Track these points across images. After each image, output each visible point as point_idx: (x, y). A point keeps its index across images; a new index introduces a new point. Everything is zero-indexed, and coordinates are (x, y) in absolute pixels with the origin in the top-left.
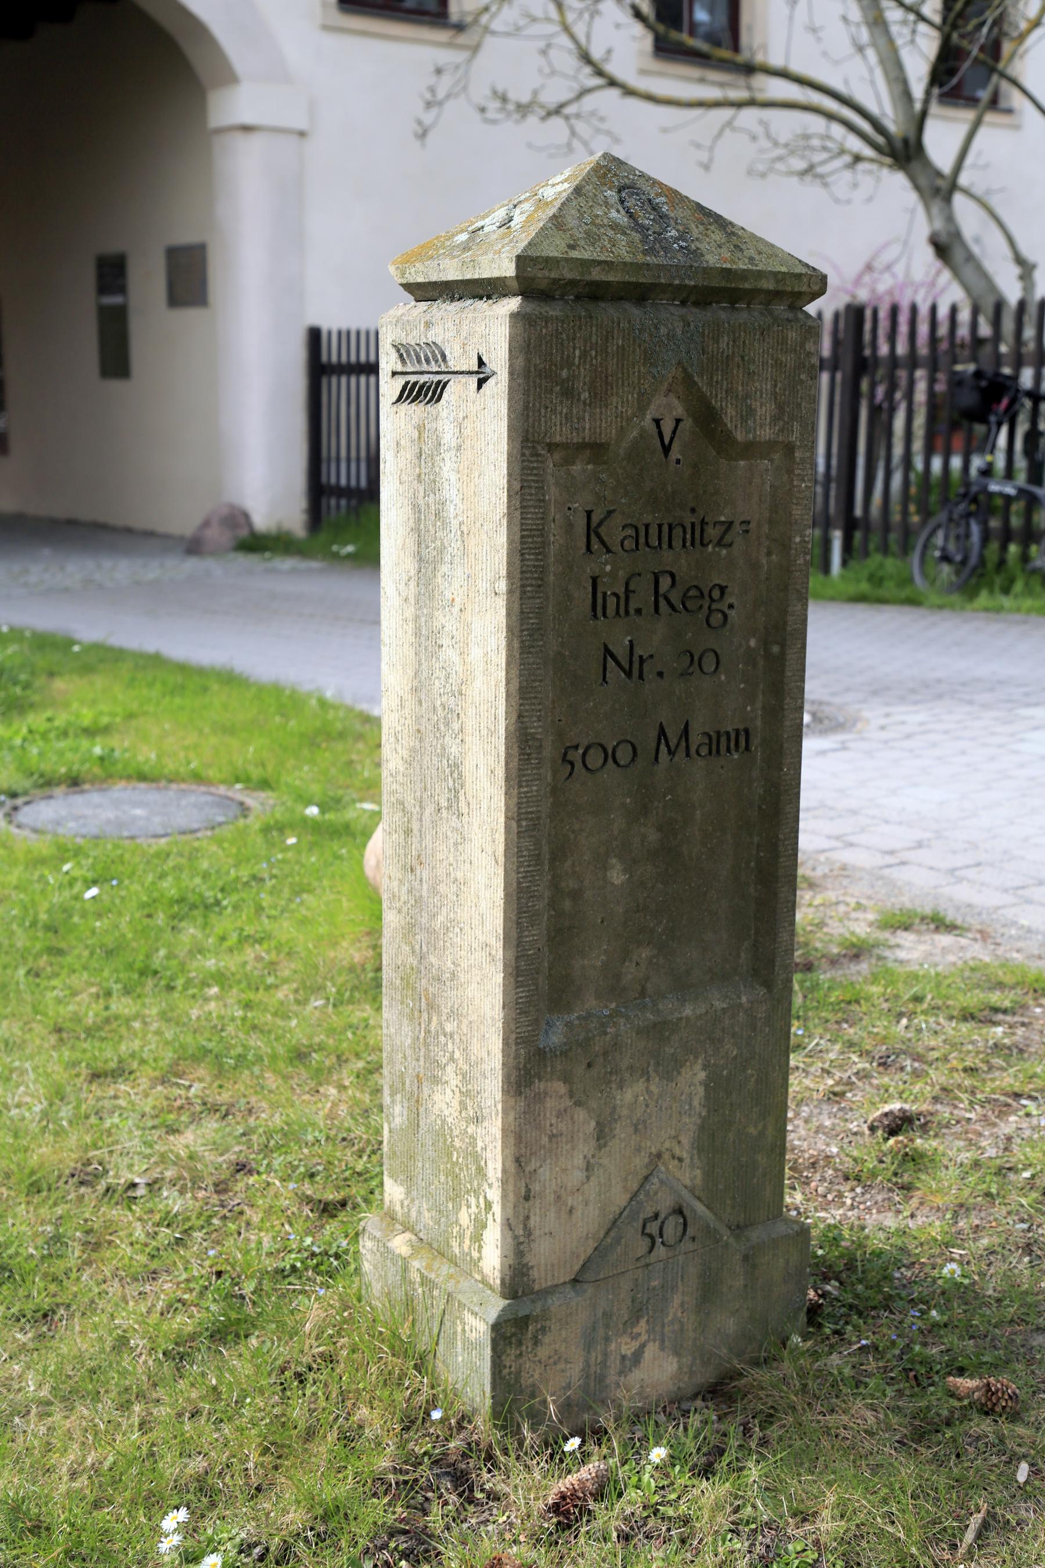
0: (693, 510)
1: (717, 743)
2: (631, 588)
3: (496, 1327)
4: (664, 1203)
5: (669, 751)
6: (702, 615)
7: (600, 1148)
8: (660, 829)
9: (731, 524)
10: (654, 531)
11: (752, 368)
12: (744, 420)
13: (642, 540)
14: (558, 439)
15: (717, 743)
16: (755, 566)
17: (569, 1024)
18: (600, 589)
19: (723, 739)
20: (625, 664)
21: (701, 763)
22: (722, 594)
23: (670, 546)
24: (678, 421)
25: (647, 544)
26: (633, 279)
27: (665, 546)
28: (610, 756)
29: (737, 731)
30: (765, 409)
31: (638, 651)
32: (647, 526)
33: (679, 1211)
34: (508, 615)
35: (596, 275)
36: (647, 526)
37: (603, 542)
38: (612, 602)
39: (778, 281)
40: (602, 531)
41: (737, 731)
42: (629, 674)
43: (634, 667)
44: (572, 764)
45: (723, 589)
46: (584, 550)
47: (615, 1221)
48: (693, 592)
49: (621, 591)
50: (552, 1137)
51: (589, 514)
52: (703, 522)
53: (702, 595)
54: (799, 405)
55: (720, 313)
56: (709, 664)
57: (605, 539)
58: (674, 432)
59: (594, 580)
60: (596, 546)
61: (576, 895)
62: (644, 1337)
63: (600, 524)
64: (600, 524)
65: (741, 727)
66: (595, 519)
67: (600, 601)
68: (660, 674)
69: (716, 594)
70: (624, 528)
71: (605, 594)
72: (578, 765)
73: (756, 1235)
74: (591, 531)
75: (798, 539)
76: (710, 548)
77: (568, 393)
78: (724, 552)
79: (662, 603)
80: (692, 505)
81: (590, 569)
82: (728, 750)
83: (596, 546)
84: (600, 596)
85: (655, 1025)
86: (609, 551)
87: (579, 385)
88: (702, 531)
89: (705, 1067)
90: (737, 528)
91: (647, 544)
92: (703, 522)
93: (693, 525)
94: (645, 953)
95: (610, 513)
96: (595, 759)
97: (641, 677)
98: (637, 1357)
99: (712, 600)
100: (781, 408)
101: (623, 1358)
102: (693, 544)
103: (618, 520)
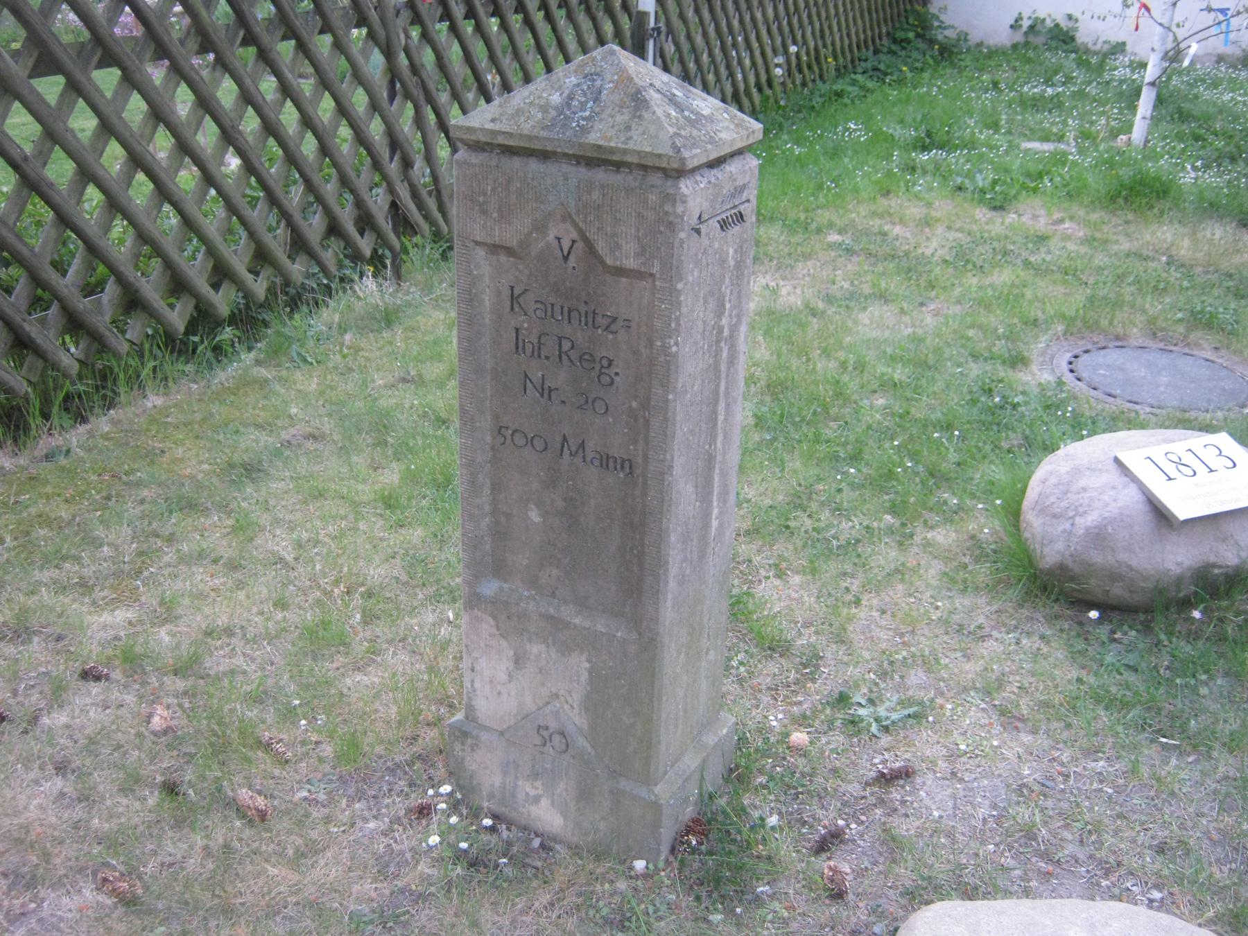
0: (586, 303)
1: (605, 461)
4: (553, 725)
5: (571, 454)
6: (594, 374)
8: (565, 500)
9: (615, 319)
10: (557, 308)
13: (549, 313)
14: (478, 239)
15: (605, 461)
16: (636, 353)
17: (501, 589)
18: (520, 338)
20: (539, 387)
22: (610, 365)
24: (574, 242)
25: (553, 316)
29: (623, 461)
30: (630, 247)
31: (547, 384)
33: (562, 734)
35: (501, 140)
38: (529, 347)
39: (640, 158)
41: (623, 461)
42: (542, 395)
43: (546, 392)
45: (610, 362)
46: (508, 310)
51: (512, 288)
52: (594, 313)
53: (594, 361)
54: (659, 249)
55: (600, 175)
58: (571, 248)
59: (517, 330)
61: (508, 516)
62: (541, 792)
63: (520, 296)
65: (626, 457)
66: (516, 292)
67: (521, 345)
69: (605, 363)
73: (624, 784)
74: (513, 298)
76: (600, 331)
77: (484, 212)
78: (611, 337)
81: (513, 323)
85: (552, 617)
89: (589, 661)
93: (586, 313)
94: (555, 572)
96: (520, 440)
98: (536, 800)
101: (527, 794)
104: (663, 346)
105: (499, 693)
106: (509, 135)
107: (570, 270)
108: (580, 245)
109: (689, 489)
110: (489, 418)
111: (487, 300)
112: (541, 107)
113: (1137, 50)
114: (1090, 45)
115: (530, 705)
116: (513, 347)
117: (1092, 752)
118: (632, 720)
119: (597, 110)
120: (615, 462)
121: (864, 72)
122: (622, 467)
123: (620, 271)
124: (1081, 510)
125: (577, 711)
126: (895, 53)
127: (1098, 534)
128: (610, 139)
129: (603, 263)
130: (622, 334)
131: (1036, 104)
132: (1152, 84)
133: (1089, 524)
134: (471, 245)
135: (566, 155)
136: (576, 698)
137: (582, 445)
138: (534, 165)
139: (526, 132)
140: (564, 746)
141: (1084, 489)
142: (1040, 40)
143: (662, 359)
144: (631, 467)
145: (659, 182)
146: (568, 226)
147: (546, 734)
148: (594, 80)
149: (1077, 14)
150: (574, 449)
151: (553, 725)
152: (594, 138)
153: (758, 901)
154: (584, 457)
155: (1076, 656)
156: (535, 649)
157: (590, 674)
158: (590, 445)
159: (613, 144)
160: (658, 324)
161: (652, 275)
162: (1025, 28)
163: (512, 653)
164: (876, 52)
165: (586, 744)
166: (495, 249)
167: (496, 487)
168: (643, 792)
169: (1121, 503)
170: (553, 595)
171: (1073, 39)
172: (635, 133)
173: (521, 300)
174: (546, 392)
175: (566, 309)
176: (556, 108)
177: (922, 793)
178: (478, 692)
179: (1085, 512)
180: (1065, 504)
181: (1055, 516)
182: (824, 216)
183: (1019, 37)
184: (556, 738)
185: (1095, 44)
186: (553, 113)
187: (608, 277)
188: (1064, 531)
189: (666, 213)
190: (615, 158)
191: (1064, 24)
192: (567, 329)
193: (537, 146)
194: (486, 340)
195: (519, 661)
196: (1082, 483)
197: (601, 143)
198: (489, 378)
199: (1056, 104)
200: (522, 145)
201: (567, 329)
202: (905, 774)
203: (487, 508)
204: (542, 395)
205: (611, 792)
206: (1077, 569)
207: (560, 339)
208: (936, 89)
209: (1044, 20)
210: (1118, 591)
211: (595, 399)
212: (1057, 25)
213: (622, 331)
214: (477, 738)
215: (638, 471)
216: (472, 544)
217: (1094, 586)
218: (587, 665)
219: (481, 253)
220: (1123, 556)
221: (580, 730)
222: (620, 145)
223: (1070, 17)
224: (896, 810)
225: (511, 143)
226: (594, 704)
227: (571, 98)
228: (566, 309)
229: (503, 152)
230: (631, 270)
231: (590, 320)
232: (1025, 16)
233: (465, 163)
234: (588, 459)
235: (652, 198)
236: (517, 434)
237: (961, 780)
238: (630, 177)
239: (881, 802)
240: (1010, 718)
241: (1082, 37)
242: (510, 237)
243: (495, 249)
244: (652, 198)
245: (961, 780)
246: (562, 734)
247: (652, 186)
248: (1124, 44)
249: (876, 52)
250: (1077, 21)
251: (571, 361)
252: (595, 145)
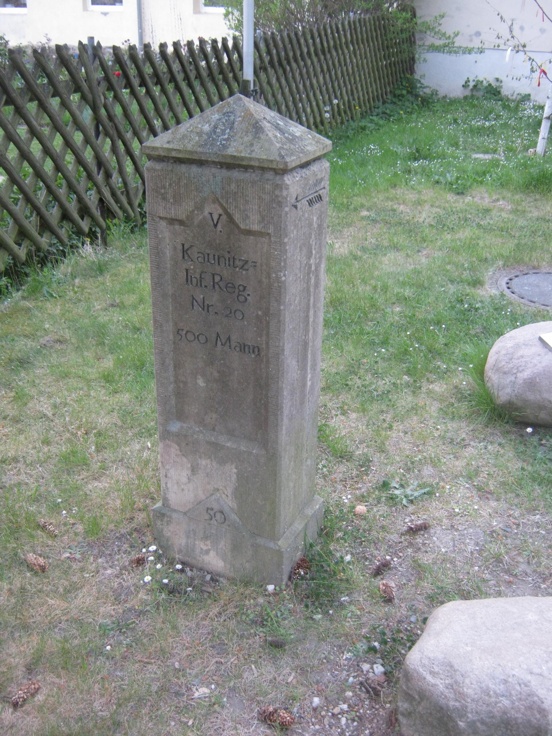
0: (229, 252)
1: (243, 348)
5: (222, 344)
7: (193, 475)
10: (211, 257)
11: (247, 198)
12: (244, 220)
13: (206, 260)
14: (161, 215)
15: (243, 348)
16: (260, 282)
17: (182, 427)
18: (189, 274)
20: (201, 304)
22: (244, 290)
23: (219, 264)
24: (220, 215)
25: (208, 261)
26: (190, 157)
29: (254, 348)
31: (207, 302)
32: (208, 254)
33: (222, 512)
35: (174, 154)
36: (208, 254)
37: (189, 256)
39: (260, 163)
42: (203, 309)
43: (206, 307)
45: (245, 288)
47: (200, 502)
48: (230, 285)
49: (198, 277)
50: (174, 462)
51: (183, 245)
52: (234, 258)
53: (235, 287)
54: (272, 218)
55: (236, 174)
56: (239, 315)
58: (219, 219)
59: (187, 270)
61: (185, 383)
62: (210, 547)
63: (188, 249)
65: (256, 345)
66: (186, 247)
67: (189, 279)
70: (198, 253)
73: (260, 541)
74: (184, 251)
75: (274, 275)
76: (237, 269)
77: (164, 199)
78: (244, 272)
80: (229, 250)
82: (249, 352)
83: (186, 258)
84: (189, 277)
85: (213, 443)
86: (192, 261)
87: (169, 196)
88: (234, 262)
89: (236, 468)
90: (250, 264)
91: (208, 261)
94: (214, 416)
96: (190, 337)
97: (208, 312)
98: (207, 552)
100: (263, 219)
101: (202, 549)
102: (229, 265)
103: (195, 250)
104: (277, 277)
105: (183, 490)
106: (179, 151)
107: (218, 232)
108: (224, 217)
109: (294, 363)
110: (171, 324)
111: (168, 253)
112: (198, 133)
113: (536, 99)
114: (509, 96)
115: (202, 497)
117: (532, 510)
118: (263, 503)
119: (232, 134)
120: (249, 348)
121: (377, 115)
122: (253, 352)
123: (249, 232)
124: (520, 369)
125: (230, 498)
126: (395, 103)
127: (531, 383)
128: (241, 152)
129: (238, 227)
130: (251, 270)
131: (480, 131)
132: (548, 118)
133: (525, 377)
134: (158, 219)
135: (214, 162)
136: (229, 491)
137: (229, 339)
138: (195, 169)
139: (189, 149)
140: (223, 520)
141: (522, 357)
142: (480, 94)
143: (276, 285)
144: (258, 351)
145: (271, 177)
146: (217, 206)
147: (212, 513)
148: (229, 116)
149: (501, 78)
150: (224, 341)
151: (216, 507)
152: (231, 151)
153: (342, 606)
154: (230, 346)
155: (519, 455)
156: (203, 462)
157: (237, 476)
158: (233, 338)
159: (242, 155)
160: (273, 264)
161: (268, 234)
162: (471, 87)
163: (190, 465)
164: (384, 103)
165: (236, 517)
166: (172, 221)
167: (177, 366)
168: (272, 545)
169: (544, 364)
170: (214, 430)
171: (499, 92)
172: (256, 148)
173: (189, 252)
174: (206, 308)
175: (216, 257)
176: (207, 134)
177: (434, 538)
178: (170, 490)
179: (523, 370)
180: (511, 365)
181: (505, 373)
182: (357, 201)
183: (468, 93)
184: (218, 515)
185: (512, 95)
186: (205, 137)
187: (242, 237)
188: (511, 381)
189: (277, 196)
190: (244, 163)
191: (494, 84)
192: (218, 269)
193: (195, 157)
194: (168, 277)
195: (194, 470)
196: (520, 353)
197: (235, 154)
198: (170, 300)
199: (491, 131)
200: (187, 157)
201: (218, 269)
202: (424, 527)
203: (172, 379)
204: (203, 309)
205: (252, 545)
206: (519, 404)
207: (213, 275)
208: (420, 123)
209: (482, 81)
210: (543, 416)
211: (235, 311)
212: (490, 85)
214: (170, 517)
215: (263, 354)
216: (163, 400)
217: (529, 413)
218: (235, 471)
219: (163, 224)
220: (546, 395)
221: (232, 509)
222: (247, 155)
223: (497, 80)
224: (420, 549)
225: (180, 156)
226: (240, 493)
227: (216, 127)
228: (216, 257)
229: (175, 162)
230: (255, 231)
232: (471, 79)
233: (152, 169)
234: (233, 347)
235: (268, 187)
236: (189, 334)
237: (457, 530)
238: (254, 175)
239: (411, 545)
240: (483, 493)
241: (505, 92)
242: (181, 212)
243: (172, 221)
244: (268, 187)
245: (457, 530)
246: (222, 512)
247: (268, 180)
248: (529, 95)
249: (384, 103)
250: (501, 82)
251: (220, 288)
252: (231, 156)
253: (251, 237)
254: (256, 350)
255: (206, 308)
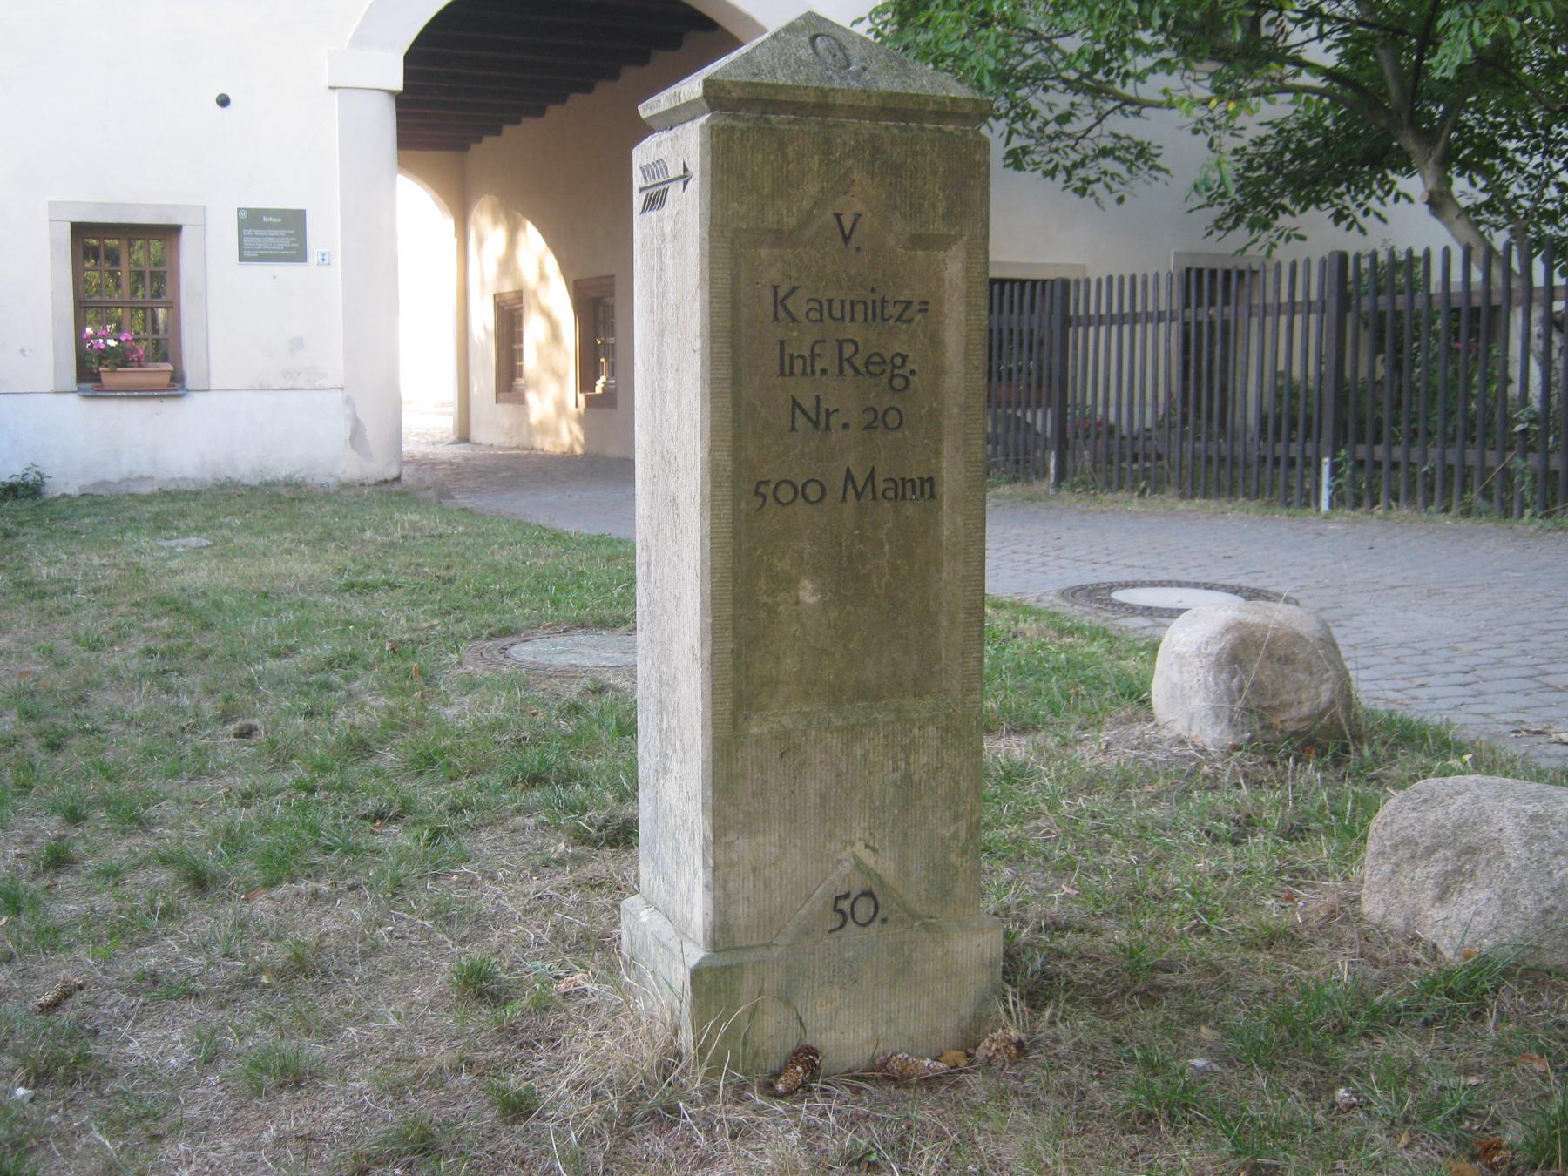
2: (817, 351)
3: (696, 974)
6: (885, 379)
9: (909, 304)
10: (837, 305)
13: (826, 313)
18: (788, 350)
19: (908, 486)
21: (887, 504)
23: (853, 319)
27: (848, 318)
28: (800, 493)
31: (824, 405)
32: (830, 301)
34: (702, 366)
36: (830, 301)
40: (789, 303)
42: (816, 424)
43: (820, 421)
44: (764, 497)
45: (904, 358)
48: (876, 359)
49: (807, 353)
51: (775, 288)
52: (883, 301)
53: (884, 362)
56: (892, 419)
57: (792, 310)
59: (782, 343)
60: (782, 315)
63: (787, 296)
64: (787, 296)
65: (925, 476)
66: (782, 293)
68: (846, 426)
69: (898, 361)
71: (791, 356)
72: (770, 499)
74: (779, 302)
76: (891, 322)
79: (846, 366)
83: (782, 315)
90: (916, 306)
91: (831, 316)
92: (883, 301)
93: (874, 302)
95: (794, 289)
96: (786, 494)
97: (828, 427)
99: (894, 367)
102: (874, 319)
116: (776, 368)
118: (952, 829)
137: (871, 477)
147: (845, 905)
150: (860, 483)
173: (789, 303)
175: (848, 305)
207: (840, 343)
211: (886, 411)
213: (919, 317)
228: (848, 305)
231: (878, 311)
234: (879, 495)
236: (783, 486)
246: (868, 894)
251: (856, 370)
253: (920, 253)
254: (927, 487)
255: (823, 424)
